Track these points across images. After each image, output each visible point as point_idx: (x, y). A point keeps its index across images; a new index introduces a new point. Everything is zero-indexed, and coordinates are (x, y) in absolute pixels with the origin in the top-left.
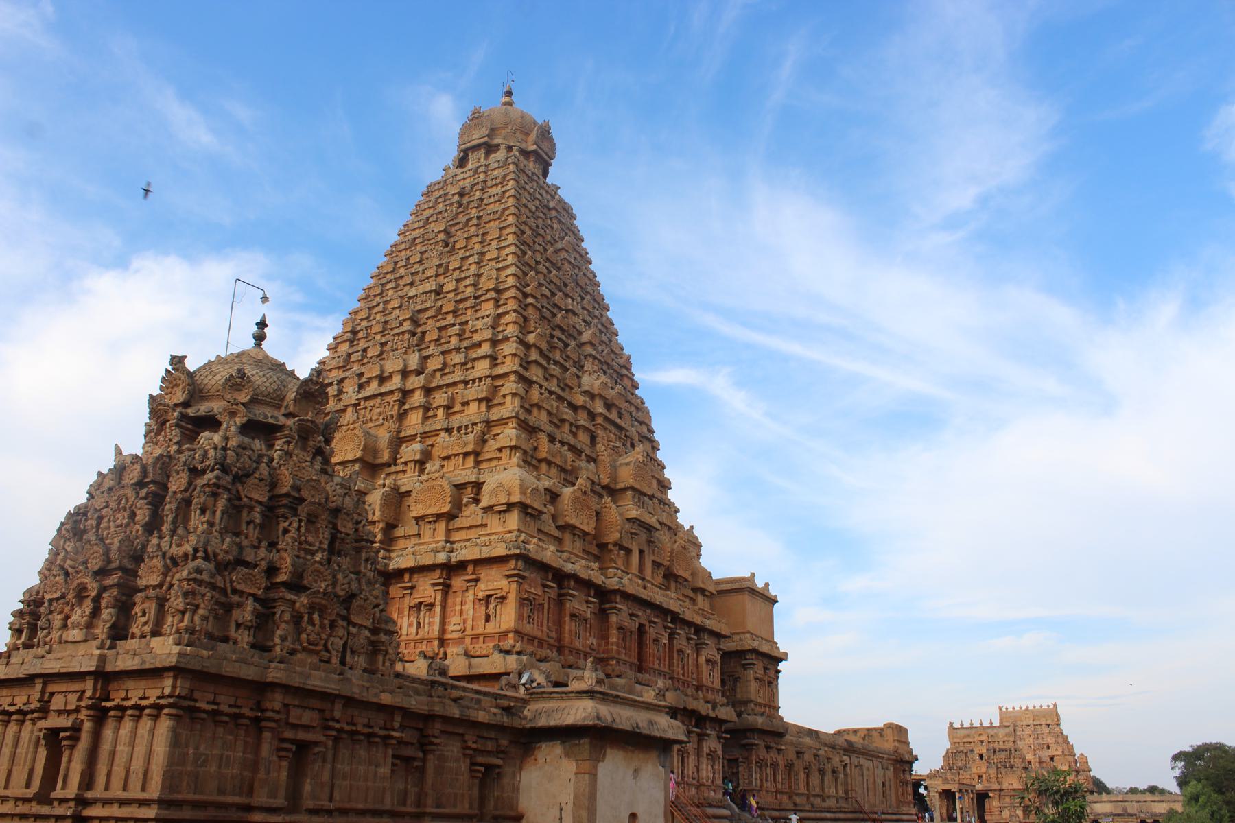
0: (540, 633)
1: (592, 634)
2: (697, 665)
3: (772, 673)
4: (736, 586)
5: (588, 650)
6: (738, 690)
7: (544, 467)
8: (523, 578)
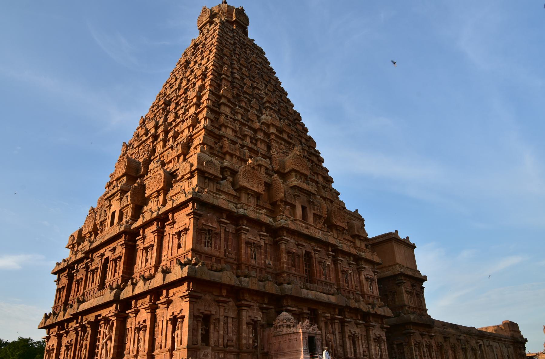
0: (219, 254)
1: (269, 258)
2: (360, 282)
3: (418, 288)
4: (386, 238)
5: (263, 266)
6: (396, 300)
7: (228, 157)
8: (200, 215)
